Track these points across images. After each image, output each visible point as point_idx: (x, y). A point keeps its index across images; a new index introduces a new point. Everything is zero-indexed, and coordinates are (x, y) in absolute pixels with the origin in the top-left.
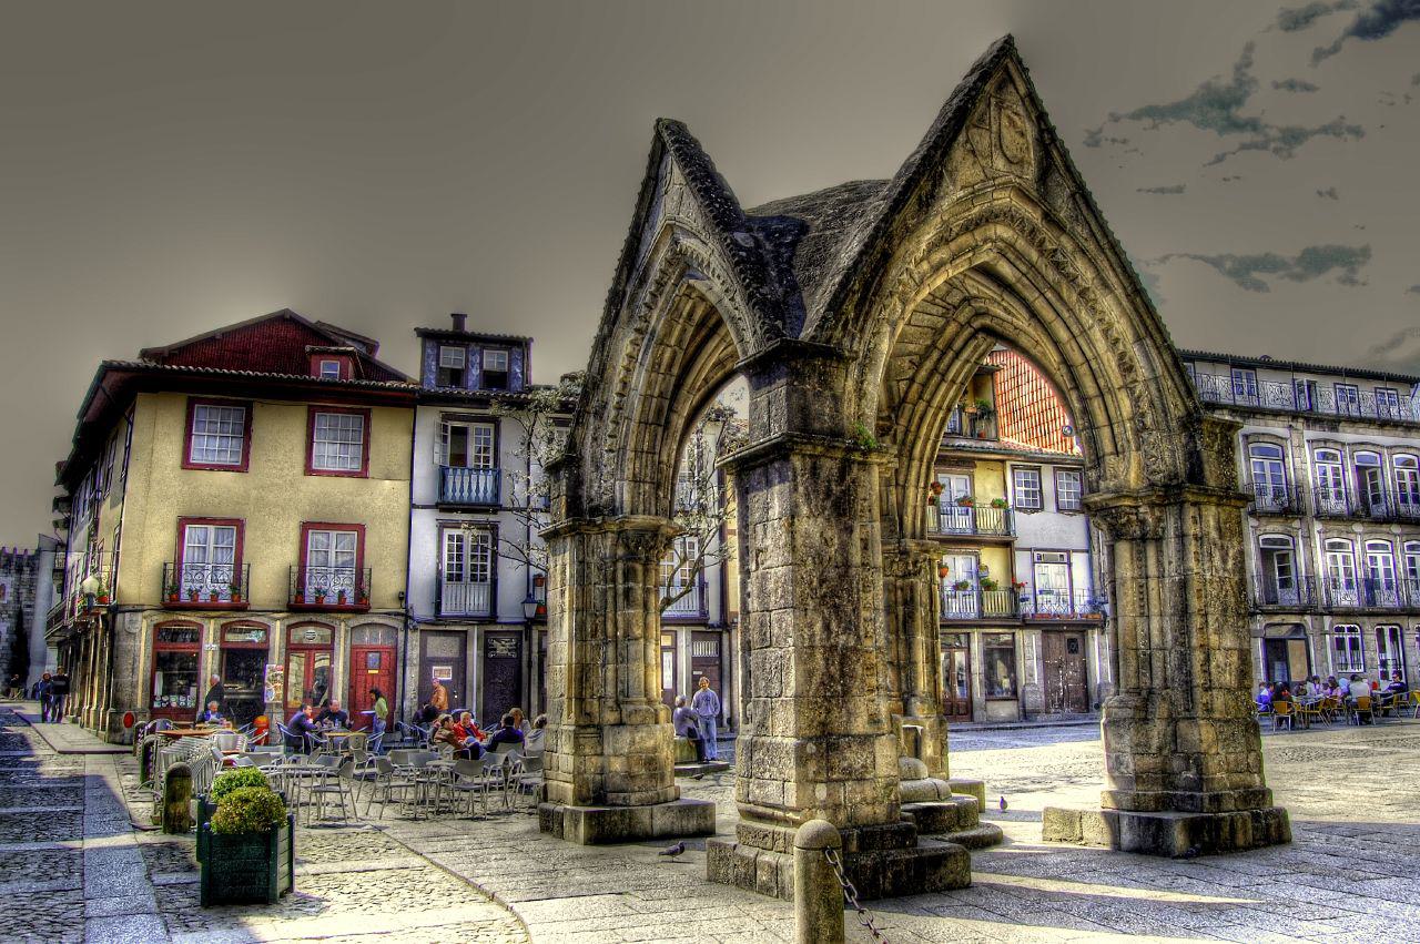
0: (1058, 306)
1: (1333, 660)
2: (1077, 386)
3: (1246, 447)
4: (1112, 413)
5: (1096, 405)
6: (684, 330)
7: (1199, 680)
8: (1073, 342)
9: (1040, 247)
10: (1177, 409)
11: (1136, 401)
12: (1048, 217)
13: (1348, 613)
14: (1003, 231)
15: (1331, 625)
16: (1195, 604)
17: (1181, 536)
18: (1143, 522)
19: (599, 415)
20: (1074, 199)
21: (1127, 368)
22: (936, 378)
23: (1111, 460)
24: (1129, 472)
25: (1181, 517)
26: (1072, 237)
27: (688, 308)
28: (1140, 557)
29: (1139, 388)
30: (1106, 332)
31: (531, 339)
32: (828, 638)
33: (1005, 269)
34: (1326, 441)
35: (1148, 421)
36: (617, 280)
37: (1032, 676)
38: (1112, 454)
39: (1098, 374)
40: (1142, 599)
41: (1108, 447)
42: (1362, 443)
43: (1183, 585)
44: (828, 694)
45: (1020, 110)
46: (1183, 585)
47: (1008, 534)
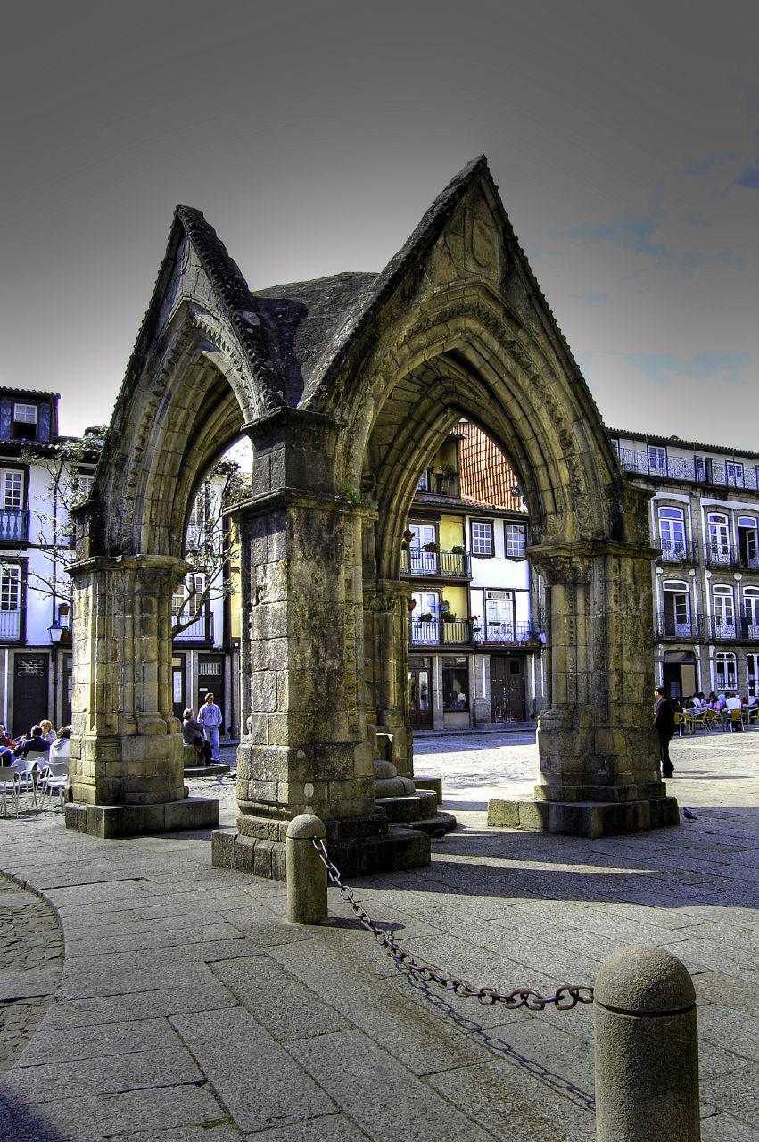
0: (514, 389)
1: (715, 680)
2: (527, 457)
3: (656, 510)
4: (554, 480)
5: (541, 473)
6: (197, 395)
7: (614, 697)
8: (525, 419)
10: (605, 479)
11: (572, 470)
12: (510, 315)
13: (727, 644)
14: (473, 324)
15: (714, 652)
16: (613, 637)
17: (605, 582)
18: (575, 570)
19: (120, 466)
20: (530, 300)
21: (566, 443)
22: (412, 444)
23: (550, 518)
24: (566, 528)
25: (605, 567)
26: (528, 332)
27: (201, 375)
28: (572, 599)
29: (576, 460)
30: (551, 413)
31: (58, 396)
32: (317, 663)
33: (471, 356)
34: (717, 507)
35: (582, 487)
36: (138, 349)
37: (481, 692)
38: (552, 513)
39: (543, 447)
40: (571, 633)
41: (549, 508)
42: (744, 510)
43: (605, 621)
44: (317, 709)
45: (490, 222)
46: (605, 621)
47: (466, 575)
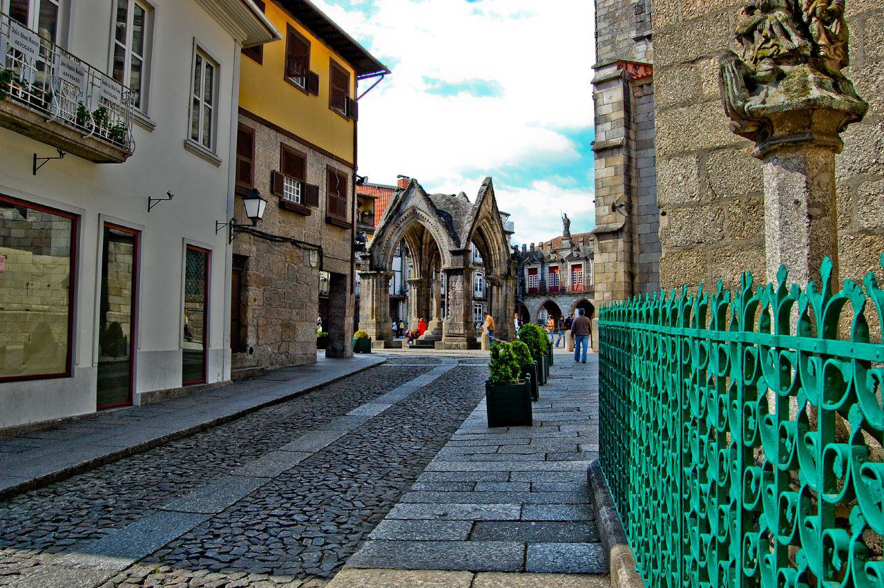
9: (489, 223)
12: (492, 217)
13: (479, 300)
16: (508, 300)
17: (507, 286)
19: (379, 245)
21: (499, 249)
25: (507, 282)
28: (498, 290)
43: (506, 296)
46: (506, 296)
